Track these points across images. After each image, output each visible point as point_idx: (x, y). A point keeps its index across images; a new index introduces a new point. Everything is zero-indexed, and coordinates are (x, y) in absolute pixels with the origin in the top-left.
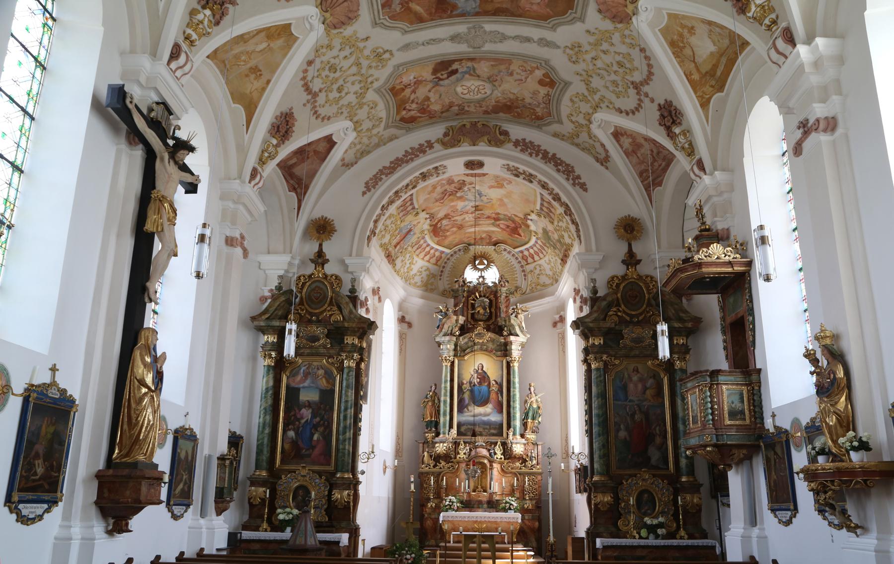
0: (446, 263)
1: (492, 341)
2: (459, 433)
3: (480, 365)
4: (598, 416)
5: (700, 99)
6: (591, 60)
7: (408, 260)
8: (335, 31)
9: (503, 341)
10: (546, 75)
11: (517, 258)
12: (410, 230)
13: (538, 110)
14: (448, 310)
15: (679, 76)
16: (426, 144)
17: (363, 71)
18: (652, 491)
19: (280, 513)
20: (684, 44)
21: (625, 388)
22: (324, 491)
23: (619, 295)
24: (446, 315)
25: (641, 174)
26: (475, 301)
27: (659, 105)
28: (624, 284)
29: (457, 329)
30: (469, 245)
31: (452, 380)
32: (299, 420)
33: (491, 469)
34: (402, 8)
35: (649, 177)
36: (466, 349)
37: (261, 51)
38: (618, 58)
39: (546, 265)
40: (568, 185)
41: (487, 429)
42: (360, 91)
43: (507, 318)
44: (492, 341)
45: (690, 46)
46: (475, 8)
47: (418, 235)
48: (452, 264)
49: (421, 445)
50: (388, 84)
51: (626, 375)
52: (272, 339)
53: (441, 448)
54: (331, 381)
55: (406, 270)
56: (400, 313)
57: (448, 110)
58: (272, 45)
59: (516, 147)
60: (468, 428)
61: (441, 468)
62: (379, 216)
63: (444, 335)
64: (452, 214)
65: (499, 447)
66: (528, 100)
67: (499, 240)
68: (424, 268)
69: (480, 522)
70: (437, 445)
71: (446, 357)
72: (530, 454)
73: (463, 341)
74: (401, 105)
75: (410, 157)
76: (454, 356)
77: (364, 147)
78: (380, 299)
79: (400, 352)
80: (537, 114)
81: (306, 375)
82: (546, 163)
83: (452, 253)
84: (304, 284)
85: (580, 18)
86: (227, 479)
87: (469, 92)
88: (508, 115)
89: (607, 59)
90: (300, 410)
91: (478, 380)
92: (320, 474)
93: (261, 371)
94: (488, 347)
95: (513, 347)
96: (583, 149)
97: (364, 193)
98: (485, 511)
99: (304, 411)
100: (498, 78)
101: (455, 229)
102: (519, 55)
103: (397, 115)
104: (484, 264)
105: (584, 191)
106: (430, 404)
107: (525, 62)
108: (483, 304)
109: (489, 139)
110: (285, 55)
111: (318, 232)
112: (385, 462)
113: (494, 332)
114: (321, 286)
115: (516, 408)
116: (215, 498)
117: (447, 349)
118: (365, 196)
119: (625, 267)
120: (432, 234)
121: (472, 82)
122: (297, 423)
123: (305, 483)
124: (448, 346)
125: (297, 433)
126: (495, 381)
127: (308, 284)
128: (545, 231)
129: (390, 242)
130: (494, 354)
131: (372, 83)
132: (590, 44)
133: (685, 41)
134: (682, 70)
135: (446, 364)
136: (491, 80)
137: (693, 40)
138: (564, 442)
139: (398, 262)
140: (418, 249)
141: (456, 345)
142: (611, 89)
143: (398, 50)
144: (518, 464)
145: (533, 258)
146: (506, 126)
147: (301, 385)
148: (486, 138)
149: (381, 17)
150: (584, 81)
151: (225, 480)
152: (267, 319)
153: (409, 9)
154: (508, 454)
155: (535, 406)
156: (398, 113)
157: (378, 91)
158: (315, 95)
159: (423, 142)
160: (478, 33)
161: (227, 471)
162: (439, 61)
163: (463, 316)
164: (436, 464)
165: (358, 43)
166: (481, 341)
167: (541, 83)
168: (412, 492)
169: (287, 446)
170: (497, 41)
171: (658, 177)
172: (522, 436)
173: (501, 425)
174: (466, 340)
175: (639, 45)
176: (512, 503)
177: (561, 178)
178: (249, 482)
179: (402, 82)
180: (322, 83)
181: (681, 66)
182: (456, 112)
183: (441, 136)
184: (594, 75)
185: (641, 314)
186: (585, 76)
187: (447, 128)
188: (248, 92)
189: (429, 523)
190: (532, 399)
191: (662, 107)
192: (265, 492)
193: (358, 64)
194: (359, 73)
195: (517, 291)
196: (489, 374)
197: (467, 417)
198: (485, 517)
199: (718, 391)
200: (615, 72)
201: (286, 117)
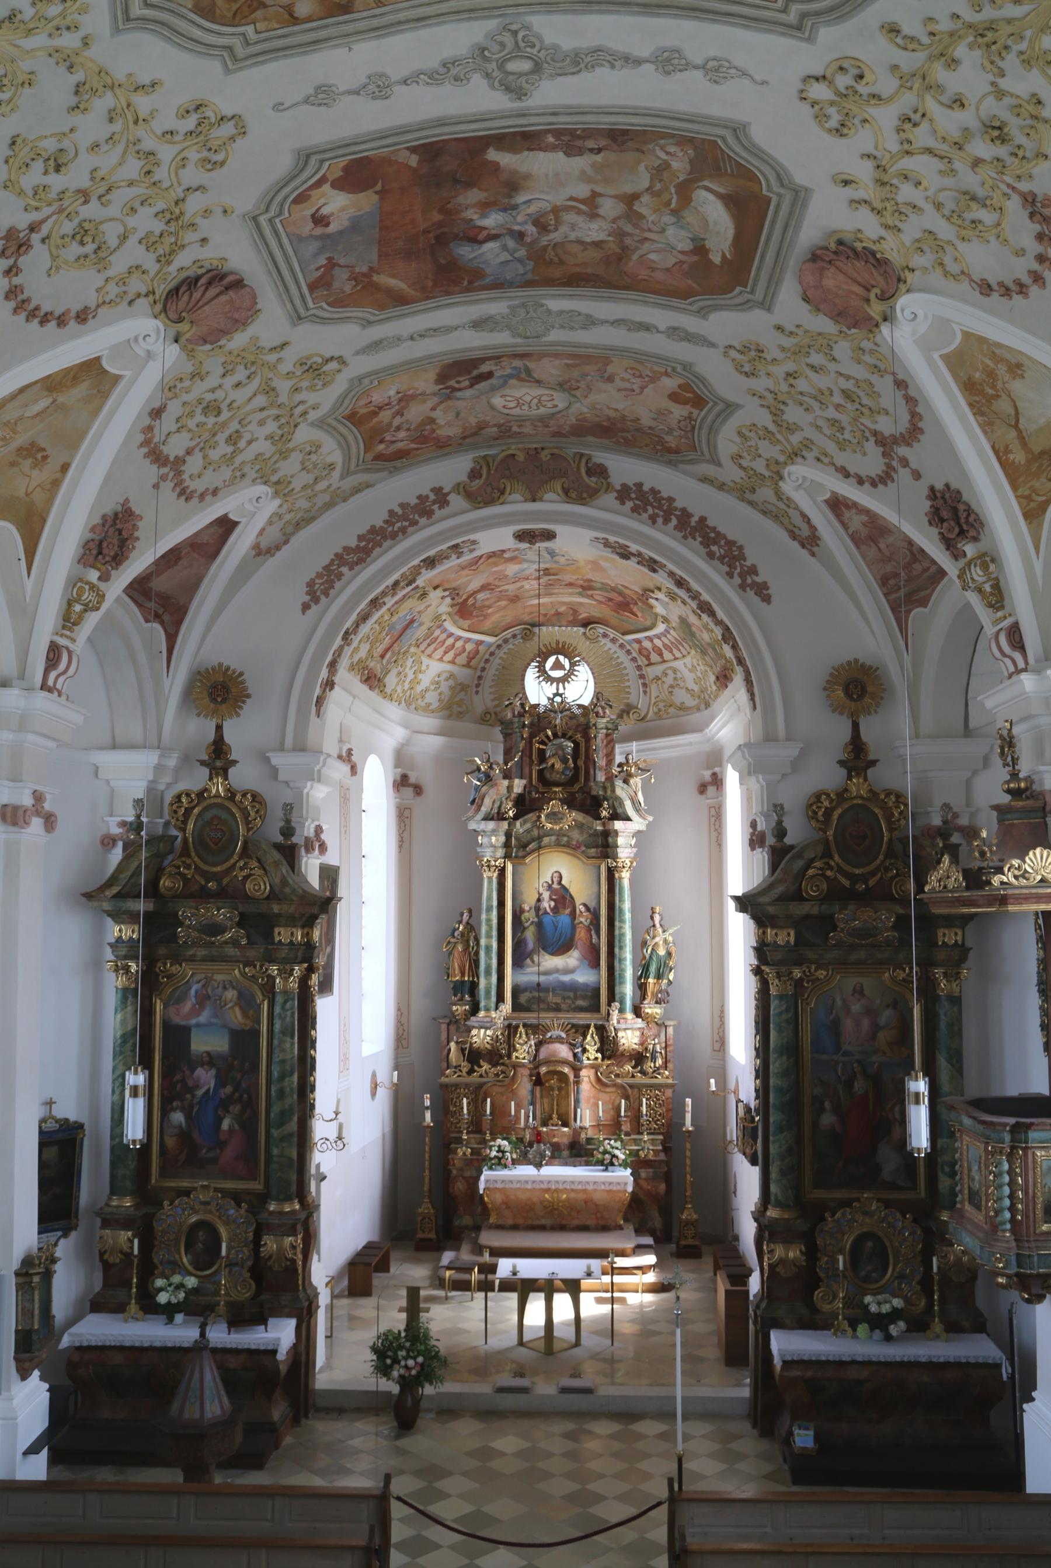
0: (487, 661)
1: (580, 826)
2: (517, 1007)
3: (556, 875)
4: (779, 1090)
5: (1024, 502)
6: (784, 375)
7: (411, 667)
9: (600, 828)
11: (628, 652)
12: (412, 621)
13: (668, 438)
14: (491, 767)
15: (980, 452)
16: (432, 497)
17: (283, 398)
19: (161, 1290)
20: (997, 391)
21: (835, 1027)
22: (246, 1233)
23: (830, 833)
24: (488, 778)
25: (884, 581)
26: (545, 744)
27: (932, 489)
28: (839, 811)
29: (510, 805)
30: (533, 625)
31: (501, 904)
32: (192, 1090)
33: (577, 1083)
35: (899, 588)
36: (529, 843)
37: (37, 415)
39: (686, 672)
40: (729, 589)
41: (569, 998)
42: (280, 432)
43: (608, 785)
44: (580, 826)
45: (1010, 396)
47: (428, 624)
48: (500, 661)
49: (444, 1027)
50: (341, 410)
51: (839, 1003)
52: (129, 933)
53: (481, 1037)
54: (251, 1012)
55: (407, 686)
56: (399, 770)
57: (476, 434)
59: (623, 503)
60: (534, 998)
61: (481, 1076)
62: (341, 649)
63: (487, 818)
64: (497, 583)
65: (592, 1037)
66: (646, 421)
67: (594, 617)
68: (444, 676)
69: (556, 1190)
70: (474, 1032)
71: (488, 861)
72: (651, 1047)
73: (519, 827)
74: (373, 436)
75: (399, 525)
76: (505, 857)
77: (298, 516)
78: (353, 770)
79: (400, 847)
81: (202, 1000)
82: (685, 537)
83: (500, 642)
84: (188, 812)
86: (37, 1312)
89: (823, 382)
90: (193, 1070)
91: (553, 904)
92: (236, 1197)
93: (111, 999)
94: (570, 838)
95: (620, 841)
96: (764, 513)
97: (306, 607)
98: (566, 1164)
99: (200, 1072)
100: (582, 385)
101: (503, 603)
102: (625, 350)
103: (365, 452)
104: (562, 667)
105: (763, 600)
106: (460, 948)
107: (638, 362)
108: (560, 752)
109: (566, 486)
110: (97, 411)
111: (213, 700)
112: (374, 1075)
113: (582, 808)
114: (225, 816)
115: (625, 959)
116: (16, 1352)
117: (492, 846)
118: (308, 612)
119: (843, 772)
120: (457, 618)
121: (524, 391)
122: (188, 1096)
123: (208, 1217)
124: (493, 839)
125: (188, 1117)
126: (585, 905)
127: (196, 811)
128: (683, 621)
129: (370, 655)
130: (583, 852)
131: (304, 414)
132: (783, 349)
133: (1000, 385)
134: (988, 439)
135: (490, 874)
136: (565, 387)
137: (1017, 387)
138: (717, 1020)
139: (391, 680)
140: (429, 645)
141: (508, 835)
142: (828, 432)
143: (357, 353)
144: (628, 1068)
145: (661, 655)
146: (601, 457)
147: (193, 1021)
148: (558, 485)
149: (311, 305)
150: (768, 407)
151: (33, 1314)
152: (115, 896)
154: (608, 1047)
155: (662, 952)
158: (180, 461)
159: (425, 491)
160: (532, 314)
161: (37, 1297)
163: (521, 778)
164: (472, 1067)
165: (263, 357)
166: (557, 827)
167: (674, 397)
168: (428, 1127)
169: (170, 1142)
170: (576, 326)
171: (919, 590)
172: (637, 1011)
173: (597, 991)
174: (528, 825)
175: (894, 374)
176: (617, 1152)
177: (714, 573)
178: (98, 1222)
180: (191, 439)
181: (985, 432)
183: (464, 478)
184: (789, 401)
185: (873, 874)
186: (771, 401)
187: (476, 461)
188: (21, 492)
189: (460, 1186)
190: (657, 939)
191: (938, 495)
192: (131, 1241)
193: (270, 390)
195: (628, 713)
196: (574, 891)
197: (529, 976)
198: (564, 1182)
199: (1026, 1164)
200: (837, 407)
201: (114, 524)
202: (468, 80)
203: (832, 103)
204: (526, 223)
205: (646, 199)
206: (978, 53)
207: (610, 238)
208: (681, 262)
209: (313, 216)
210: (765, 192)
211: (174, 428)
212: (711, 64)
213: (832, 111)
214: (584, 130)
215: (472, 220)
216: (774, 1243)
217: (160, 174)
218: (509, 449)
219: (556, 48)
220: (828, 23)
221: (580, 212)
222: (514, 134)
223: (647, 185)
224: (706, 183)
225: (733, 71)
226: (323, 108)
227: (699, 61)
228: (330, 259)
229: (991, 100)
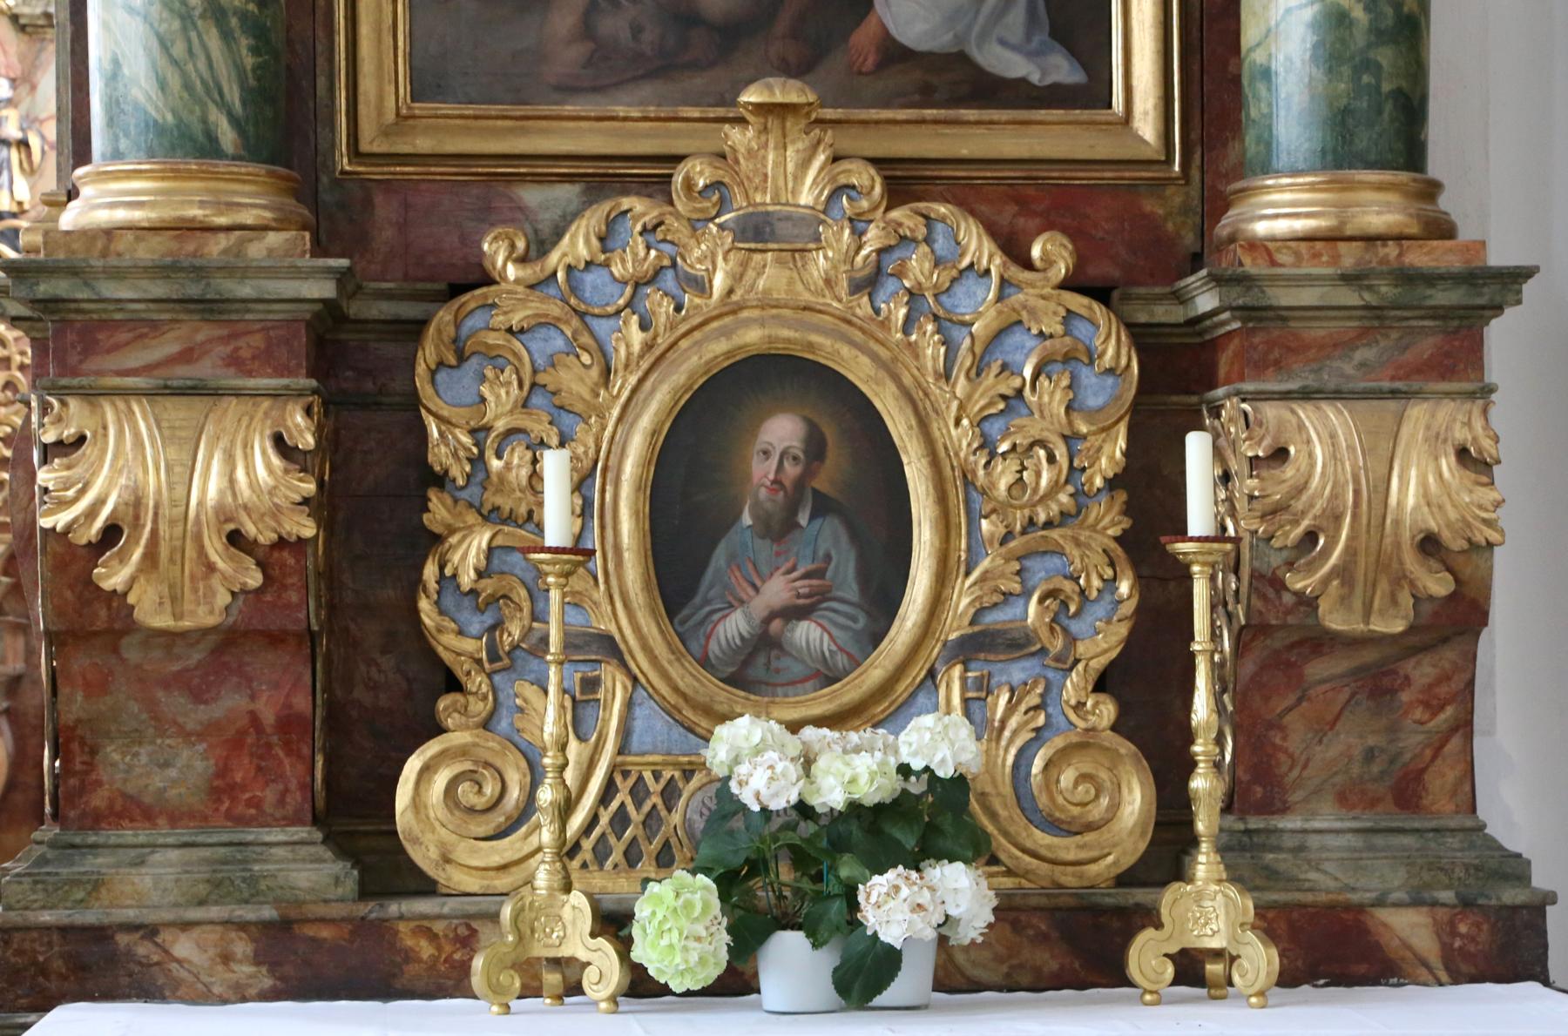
18: (859, 370)
216: (91, 395)
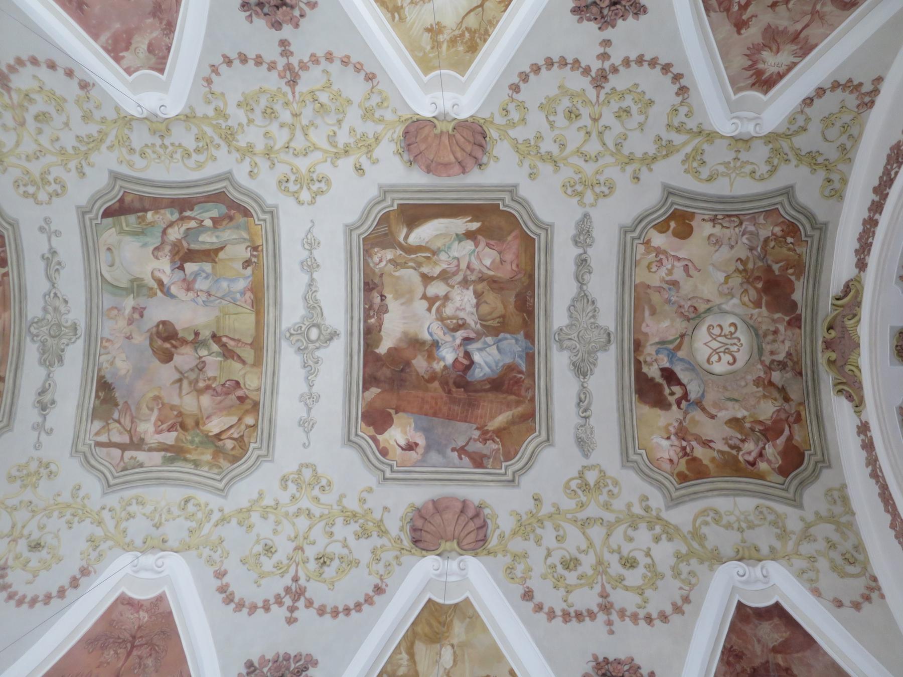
8: (493, 542)
10: (662, 228)
13: (764, 233)
34: (493, 440)
38: (560, 120)
45: (461, 22)
46: (517, 340)
58: (455, 641)
80: (780, 234)
85: (511, 192)
87: (727, 351)
88: (799, 285)
110: (485, 629)
131: (647, 509)
133: (457, 33)
136: (692, 315)
137: (450, 20)
143: (586, 456)
153: (500, 432)
156: (761, 476)
157: (674, 502)
158: (606, 608)
162: (634, 397)
165: (540, 514)
170: (590, 308)
179: (671, 461)
181: (498, 22)
182: (789, 375)
194: (610, 528)
202: (318, 357)
203: (309, 189)
204: (453, 337)
205: (425, 270)
206: (239, 137)
207: (471, 288)
208: (488, 245)
209: (403, 449)
210: (395, 207)
211: (562, 592)
212: (307, 246)
213: (314, 188)
214: (365, 304)
215: (445, 366)
217: (317, 511)
218: (822, 364)
219: (303, 317)
220: (264, 202)
221: (443, 305)
222: (365, 338)
223: (412, 270)
224: (401, 239)
225: (309, 237)
226: (315, 426)
227: (307, 253)
228: (453, 450)
229: (257, 122)
